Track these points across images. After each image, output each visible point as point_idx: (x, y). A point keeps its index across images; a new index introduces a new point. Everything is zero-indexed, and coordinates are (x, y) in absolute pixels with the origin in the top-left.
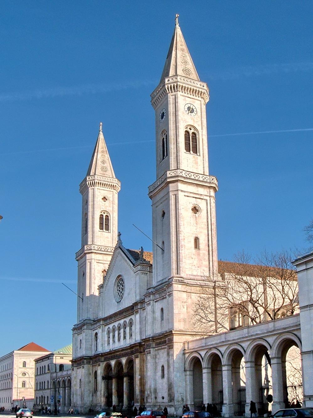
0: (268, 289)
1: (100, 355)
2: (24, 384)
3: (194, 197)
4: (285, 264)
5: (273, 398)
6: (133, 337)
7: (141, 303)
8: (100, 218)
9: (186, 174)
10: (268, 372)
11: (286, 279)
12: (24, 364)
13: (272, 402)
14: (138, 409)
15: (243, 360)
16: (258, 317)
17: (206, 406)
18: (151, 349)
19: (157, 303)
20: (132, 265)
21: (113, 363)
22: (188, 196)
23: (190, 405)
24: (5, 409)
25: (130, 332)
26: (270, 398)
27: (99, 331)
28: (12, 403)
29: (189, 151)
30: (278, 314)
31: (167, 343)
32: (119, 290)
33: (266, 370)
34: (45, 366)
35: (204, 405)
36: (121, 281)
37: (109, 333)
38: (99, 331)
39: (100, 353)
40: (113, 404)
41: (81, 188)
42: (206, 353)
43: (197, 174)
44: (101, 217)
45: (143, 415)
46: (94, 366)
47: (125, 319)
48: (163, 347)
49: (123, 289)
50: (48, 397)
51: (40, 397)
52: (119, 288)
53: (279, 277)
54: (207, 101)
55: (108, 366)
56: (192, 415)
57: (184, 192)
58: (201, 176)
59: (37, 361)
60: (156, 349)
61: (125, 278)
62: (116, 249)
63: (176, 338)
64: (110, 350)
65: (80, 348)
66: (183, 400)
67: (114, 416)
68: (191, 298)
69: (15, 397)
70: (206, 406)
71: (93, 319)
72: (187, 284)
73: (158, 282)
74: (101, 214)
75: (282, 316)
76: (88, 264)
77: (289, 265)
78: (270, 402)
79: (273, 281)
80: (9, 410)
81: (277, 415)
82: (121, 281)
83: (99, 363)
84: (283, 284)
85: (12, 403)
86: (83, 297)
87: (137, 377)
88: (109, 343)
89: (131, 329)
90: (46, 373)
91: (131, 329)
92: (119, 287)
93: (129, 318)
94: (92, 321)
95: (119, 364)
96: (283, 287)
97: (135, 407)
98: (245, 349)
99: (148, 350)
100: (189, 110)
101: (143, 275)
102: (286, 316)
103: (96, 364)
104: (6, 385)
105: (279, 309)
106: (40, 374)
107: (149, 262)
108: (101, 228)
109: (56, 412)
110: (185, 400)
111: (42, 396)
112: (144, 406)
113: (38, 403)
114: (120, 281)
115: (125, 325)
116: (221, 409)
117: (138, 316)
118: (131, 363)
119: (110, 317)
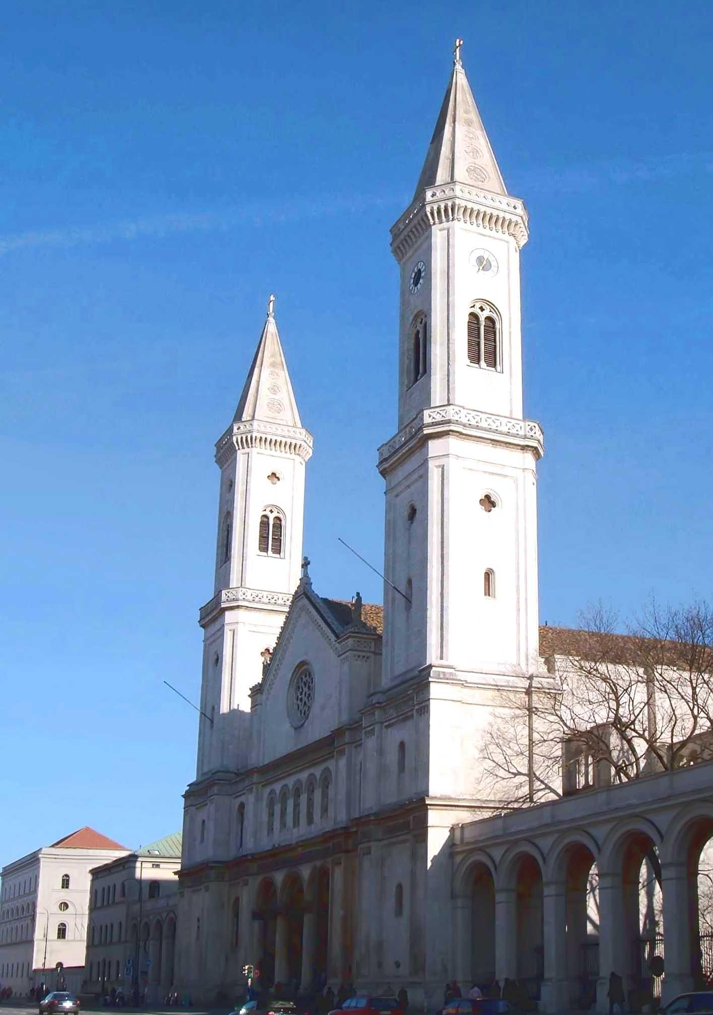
0: (658, 695)
1: (250, 858)
2: (62, 932)
4: (700, 633)
5: (666, 965)
6: (331, 813)
8: (262, 523)
9: (469, 417)
10: (651, 899)
11: (703, 669)
12: (66, 883)
13: (663, 976)
14: (336, 992)
15: (594, 870)
16: (631, 764)
17: (502, 984)
18: (373, 844)
19: (389, 730)
20: (333, 638)
21: (279, 877)
24: (14, 991)
26: (657, 965)
27: (250, 799)
28: (31, 979)
29: (478, 361)
30: (682, 757)
33: (650, 895)
35: (497, 983)
38: (250, 799)
39: (249, 852)
40: (277, 979)
41: (218, 452)
42: (506, 852)
43: (494, 417)
44: (264, 524)
45: (349, 1007)
47: (312, 771)
48: (401, 838)
50: (118, 963)
52: (301, 694)
53: (684, 665)
54: (523, 241)
55: (268, 887)
56: (467, 1009)
59: (96, 873)
60: (386, 842)
61: (317, 668)
62: (297, 597)
63: (434, 817)
64: (274, 845)
65: (202, 840)
67: (277, 1010)
69: (37, 965)
70: (502, 984)
72: (464, 684)
74: (264, 513)
75: (689, 762)
77: (708, 636)
78: (659, 975)
79: (671, 673)
80: (24, 995)
81: (672, 1008)
84: (694, 682)
85: (31, 979)
86: (212, 715)
87: (337, 912)
88: (271, 830)
89: (325, 795)
91: (325, 795)
93: (322, 767)
94: (233, 775)
95: (294, 880)
96: (694, 689)
97: (330, 988)
98: (600, 843)
99: (366, 845)
100: (480, 260)
101: (359, 662)
102: (699, 760)
104: (19, 933)
105: (683, 744)
106: (103, 906)
107: (375, 629)
108: (263, 547)
109: (137, 1002)
111: (104, 961)
112: (351, 985)
115: (311, 783)
116: (539, 991)
117: (343, 762)
118: (322, 878)
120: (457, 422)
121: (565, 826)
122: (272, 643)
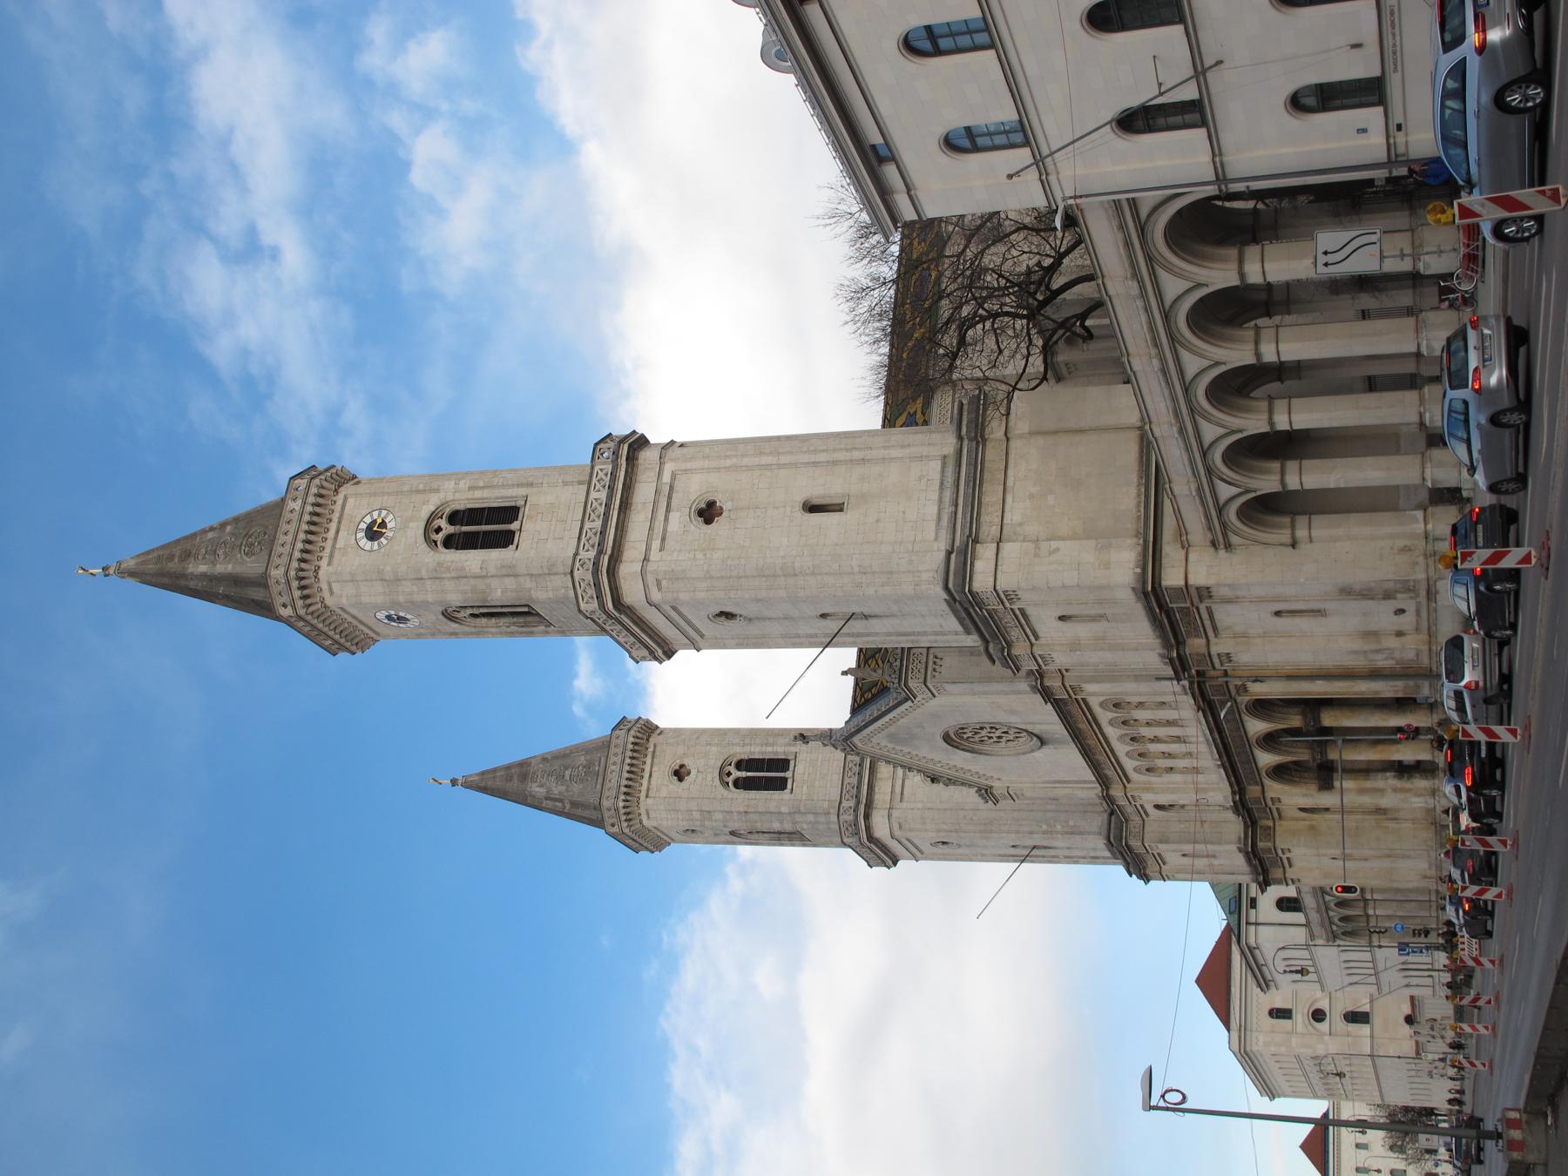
3: (666, 519)
6: (1169, 698)
7: (1042, 677)
20: (909, 703)
21: (1266, 759)
22: (663, 539)
55: (1279, 772)
57: (648, 549)
68: (1021, 524)
71: (1106, 816)
88: (1196, 770)
89: (1140, 705)
98: (1207, 363)
101: (943, 670)
110: (1408, 543)
115: (1124, 723)
117: (1090, 688)
118: (1262, 707)
119: (1095, 766)
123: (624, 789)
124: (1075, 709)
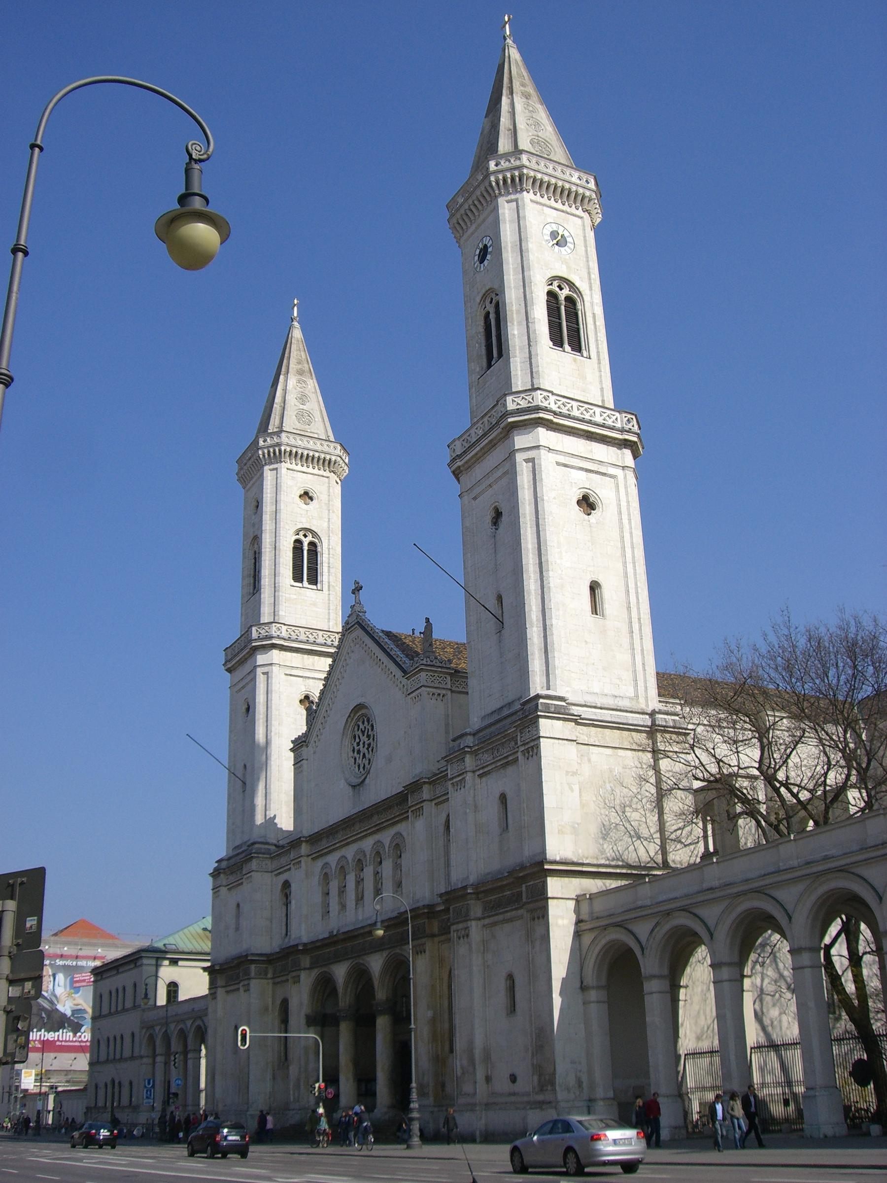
1: (300, 948)
3: (581, 469)
9: (559, 403)
19: (484, 779)
23: (604, 1099)
25: (394, 877)
29: (561, 345)
31: (524, 900)
32: (356, 748)
34: (124, 988)
36: (363, 723)
37: (326, 878)
42: (656, 926)
43: (586, 406)
46: (278, 983)
47: (377, 837)
48: (508, 915)
49: (369, 745)
51: (106, 1085)
52: (358, 744)
58: (598, 410)
61: (378, 712)
62: (348, 628)
66: (580, 1083)
71: (275, 842)
72: (577, 721)
73: (483, 718)
76: (261, 679)
82: (363, 723)
83: (294, 974)
86: (244, 775)
89: (397, 867)
90: (128, 1010)
91: (397, 867)
92: (357, 740)
93: (392, 831)
94: (274, 848)
95: (361, 975)
99: (461, 926)
101: (434, 701)
103: (284, 978)
107: (450, 661)
111: (113, 1081)
113: (101, 1103)
114: (360, 723)
115: (378, 853)
117: (420, 825)
120: (546, 409)
121: (735, 890)
122: (315, 689)
123: (294, 450)
124: (396, 811)
